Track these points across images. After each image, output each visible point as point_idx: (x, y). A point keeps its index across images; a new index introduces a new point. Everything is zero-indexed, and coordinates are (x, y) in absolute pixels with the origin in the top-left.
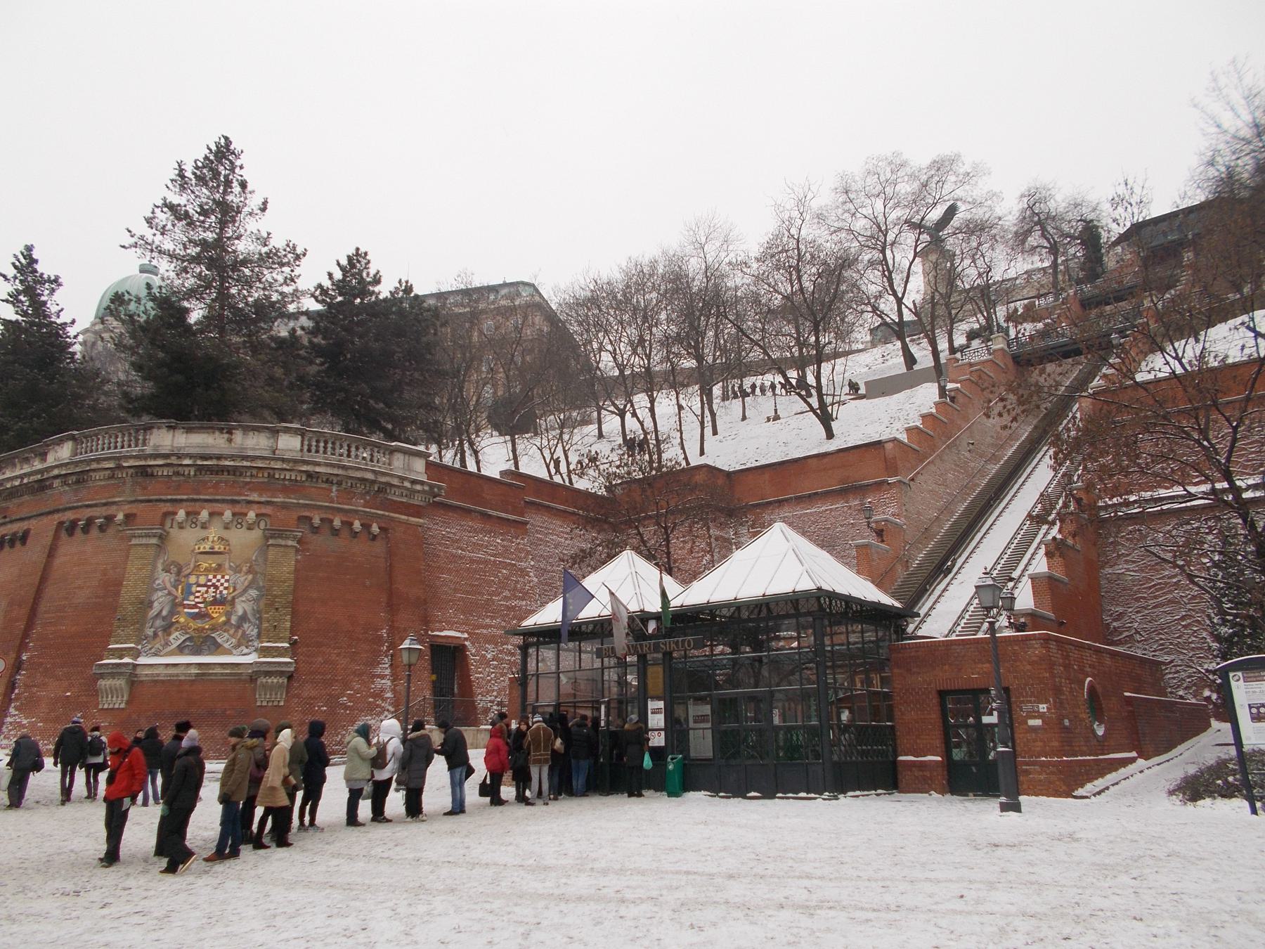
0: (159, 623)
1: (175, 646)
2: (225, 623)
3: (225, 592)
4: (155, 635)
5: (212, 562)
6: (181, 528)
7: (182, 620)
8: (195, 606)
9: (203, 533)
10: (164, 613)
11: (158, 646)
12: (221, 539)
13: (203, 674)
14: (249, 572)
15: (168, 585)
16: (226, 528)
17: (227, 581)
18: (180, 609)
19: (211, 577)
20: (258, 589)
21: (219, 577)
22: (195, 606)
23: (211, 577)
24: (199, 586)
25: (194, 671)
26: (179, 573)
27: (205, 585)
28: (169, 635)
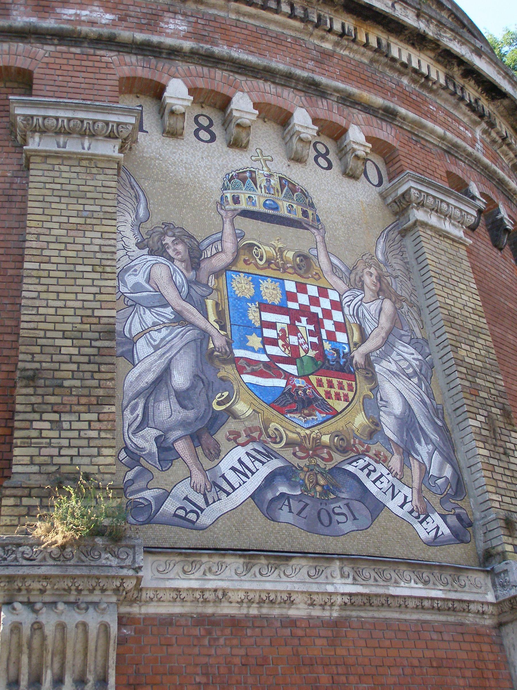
0: (166, 410)
1: (242, 494)
2: (371, 434)
3: (341, 337)
4: (166, 452)
5: (287, 243)
6: (174, 134)
7: (242, 407)
8: (270, 368)
9: (239, 161)
10: (180, 379)
11: (183, 489)
12: (288, 187)
13: (368, 600)
14: (382, 291)
15: (171, 294)
16: (297, 159)
17: (337, 305)
18: (228, 371)
19: (291, 287)
20: (414, 342)
21: (313, 291)
22: (270, 368)
23: (291, 287)
24: (264, 307)
25: (341, 584)
26: (195, 260)
27: (281, 310)
28: (215, 454)
